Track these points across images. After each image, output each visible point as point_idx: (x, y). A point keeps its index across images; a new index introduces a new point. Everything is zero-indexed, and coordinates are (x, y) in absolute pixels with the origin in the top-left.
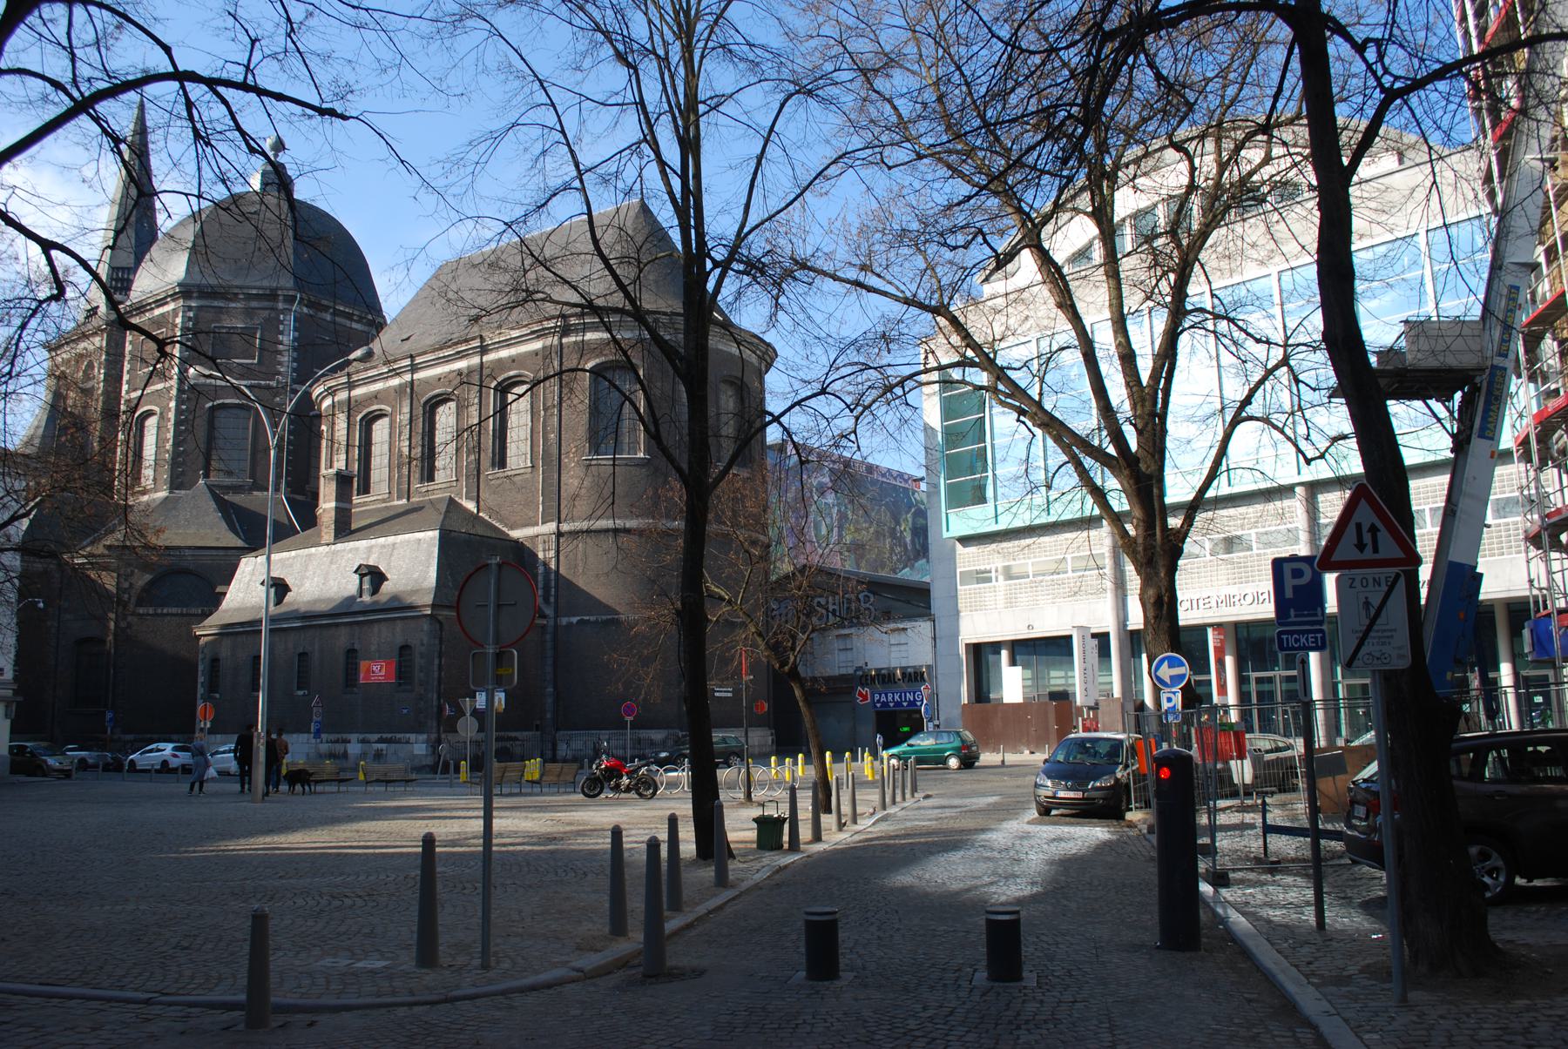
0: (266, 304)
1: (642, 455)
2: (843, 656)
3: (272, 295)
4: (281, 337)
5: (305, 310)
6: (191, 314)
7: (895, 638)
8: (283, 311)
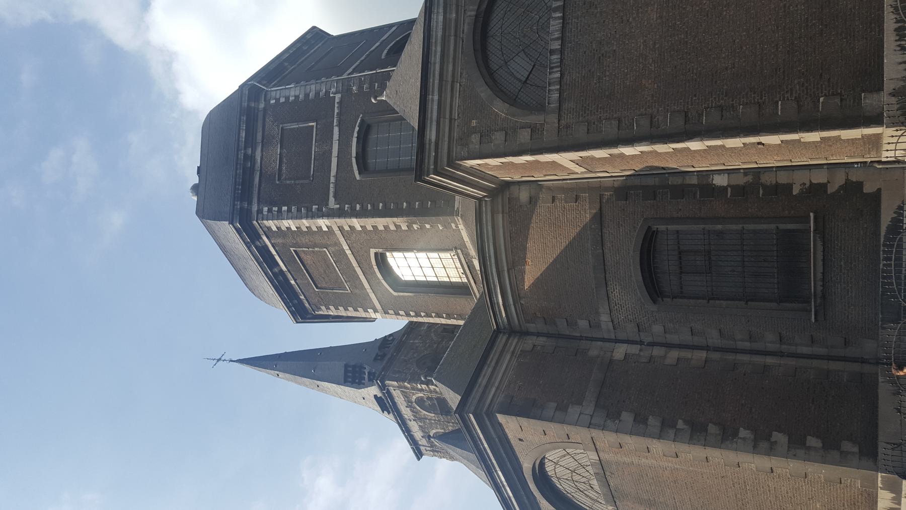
4: (292, 99)
8: (267, 101)
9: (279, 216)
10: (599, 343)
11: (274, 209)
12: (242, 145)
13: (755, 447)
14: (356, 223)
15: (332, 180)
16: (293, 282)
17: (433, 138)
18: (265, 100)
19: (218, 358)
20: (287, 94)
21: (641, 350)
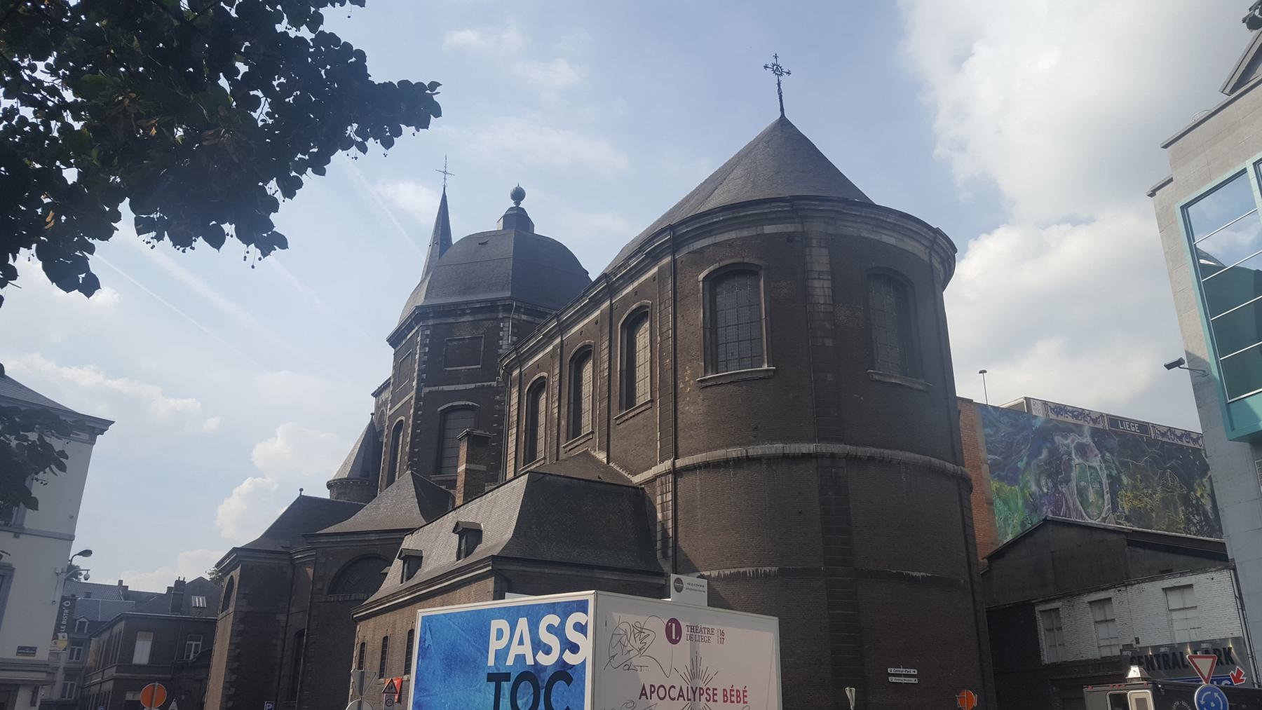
0: (488, 315)
1: (765, 367)
2: (1103, 631)
3: (492, 307)
4: (501, 342)
5: (524, 317)
6: (428, 332)
7: (1175, 600)
8: (503, 320)
9: (423, 345)
10: (287, 606)
11: (428, 339)
12: (471, 306)
13: (227, 682)
14: (412, 411)
15: (441, 388)
16: (404, 342)
17: (322, 541)
18: (504, 318)
19: (443, 175)
20: (504, 339)
21: (283, 627)
